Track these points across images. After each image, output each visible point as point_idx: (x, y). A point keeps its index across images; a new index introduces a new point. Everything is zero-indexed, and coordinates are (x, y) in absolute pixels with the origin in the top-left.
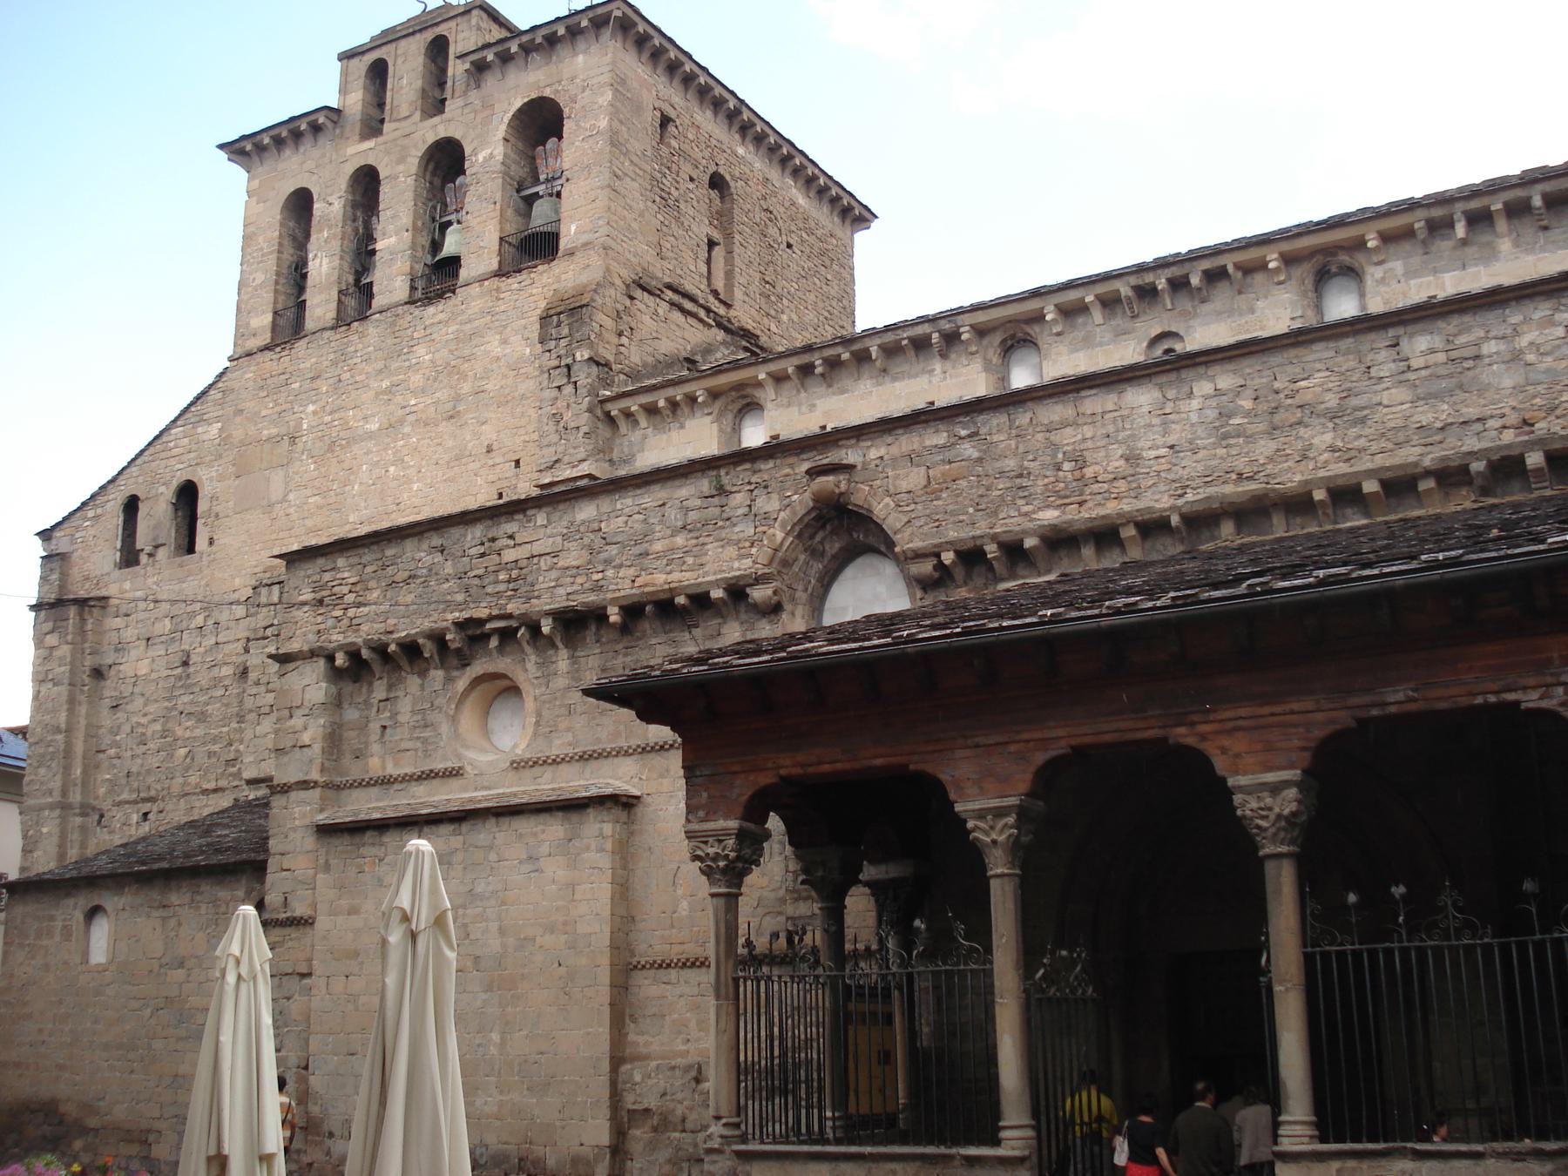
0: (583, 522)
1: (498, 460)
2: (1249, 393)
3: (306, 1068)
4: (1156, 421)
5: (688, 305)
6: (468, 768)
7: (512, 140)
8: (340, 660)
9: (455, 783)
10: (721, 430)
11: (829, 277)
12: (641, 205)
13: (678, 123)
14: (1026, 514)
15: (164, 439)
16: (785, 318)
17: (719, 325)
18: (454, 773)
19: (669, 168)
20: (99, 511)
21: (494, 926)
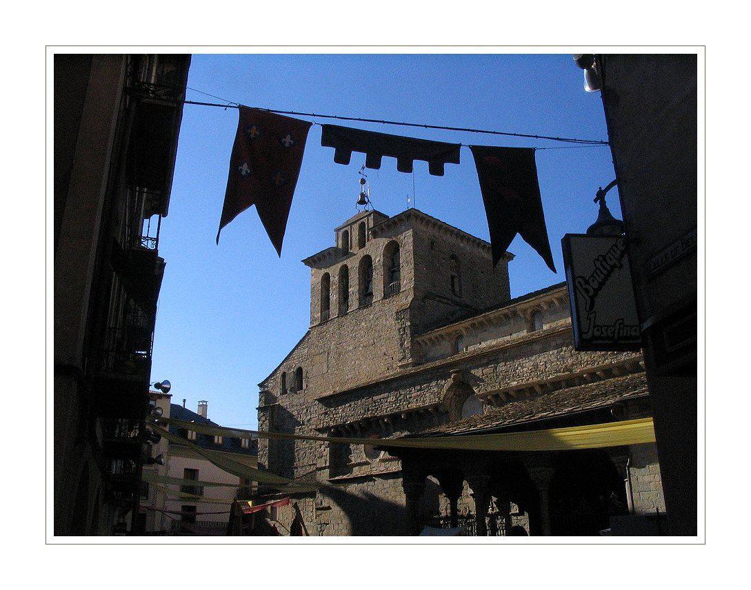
5: (444, 301)
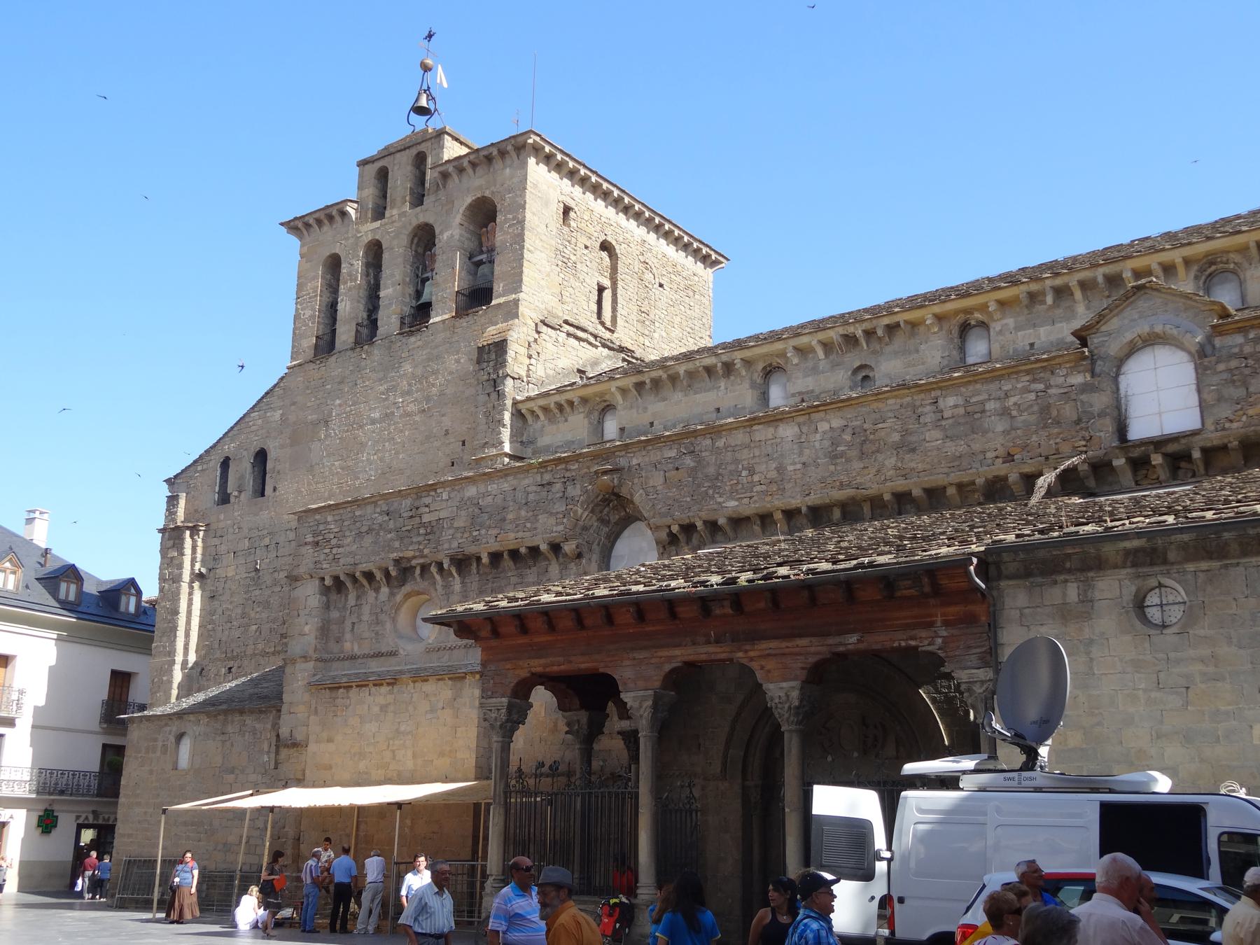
0: (469, 498)
1: (453, 440)
2: (849, 430)
3: (299, 839)
4: (795, 446)
6: (401, 651)
7: (466, 224)
8: (328, 582)
9: (393, 660)
10: (590, 423)
11: (692, 304)
12: (548, 269)
13: (576, 210)
14: (720, 503)
15: (247, 420)
16: (656, 335)
17: (604, 346)
18: (393, 654)
19: (569, 242)
20: (205, 466)
21: (410, 753)
